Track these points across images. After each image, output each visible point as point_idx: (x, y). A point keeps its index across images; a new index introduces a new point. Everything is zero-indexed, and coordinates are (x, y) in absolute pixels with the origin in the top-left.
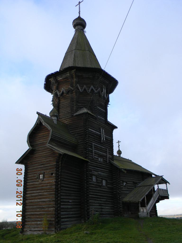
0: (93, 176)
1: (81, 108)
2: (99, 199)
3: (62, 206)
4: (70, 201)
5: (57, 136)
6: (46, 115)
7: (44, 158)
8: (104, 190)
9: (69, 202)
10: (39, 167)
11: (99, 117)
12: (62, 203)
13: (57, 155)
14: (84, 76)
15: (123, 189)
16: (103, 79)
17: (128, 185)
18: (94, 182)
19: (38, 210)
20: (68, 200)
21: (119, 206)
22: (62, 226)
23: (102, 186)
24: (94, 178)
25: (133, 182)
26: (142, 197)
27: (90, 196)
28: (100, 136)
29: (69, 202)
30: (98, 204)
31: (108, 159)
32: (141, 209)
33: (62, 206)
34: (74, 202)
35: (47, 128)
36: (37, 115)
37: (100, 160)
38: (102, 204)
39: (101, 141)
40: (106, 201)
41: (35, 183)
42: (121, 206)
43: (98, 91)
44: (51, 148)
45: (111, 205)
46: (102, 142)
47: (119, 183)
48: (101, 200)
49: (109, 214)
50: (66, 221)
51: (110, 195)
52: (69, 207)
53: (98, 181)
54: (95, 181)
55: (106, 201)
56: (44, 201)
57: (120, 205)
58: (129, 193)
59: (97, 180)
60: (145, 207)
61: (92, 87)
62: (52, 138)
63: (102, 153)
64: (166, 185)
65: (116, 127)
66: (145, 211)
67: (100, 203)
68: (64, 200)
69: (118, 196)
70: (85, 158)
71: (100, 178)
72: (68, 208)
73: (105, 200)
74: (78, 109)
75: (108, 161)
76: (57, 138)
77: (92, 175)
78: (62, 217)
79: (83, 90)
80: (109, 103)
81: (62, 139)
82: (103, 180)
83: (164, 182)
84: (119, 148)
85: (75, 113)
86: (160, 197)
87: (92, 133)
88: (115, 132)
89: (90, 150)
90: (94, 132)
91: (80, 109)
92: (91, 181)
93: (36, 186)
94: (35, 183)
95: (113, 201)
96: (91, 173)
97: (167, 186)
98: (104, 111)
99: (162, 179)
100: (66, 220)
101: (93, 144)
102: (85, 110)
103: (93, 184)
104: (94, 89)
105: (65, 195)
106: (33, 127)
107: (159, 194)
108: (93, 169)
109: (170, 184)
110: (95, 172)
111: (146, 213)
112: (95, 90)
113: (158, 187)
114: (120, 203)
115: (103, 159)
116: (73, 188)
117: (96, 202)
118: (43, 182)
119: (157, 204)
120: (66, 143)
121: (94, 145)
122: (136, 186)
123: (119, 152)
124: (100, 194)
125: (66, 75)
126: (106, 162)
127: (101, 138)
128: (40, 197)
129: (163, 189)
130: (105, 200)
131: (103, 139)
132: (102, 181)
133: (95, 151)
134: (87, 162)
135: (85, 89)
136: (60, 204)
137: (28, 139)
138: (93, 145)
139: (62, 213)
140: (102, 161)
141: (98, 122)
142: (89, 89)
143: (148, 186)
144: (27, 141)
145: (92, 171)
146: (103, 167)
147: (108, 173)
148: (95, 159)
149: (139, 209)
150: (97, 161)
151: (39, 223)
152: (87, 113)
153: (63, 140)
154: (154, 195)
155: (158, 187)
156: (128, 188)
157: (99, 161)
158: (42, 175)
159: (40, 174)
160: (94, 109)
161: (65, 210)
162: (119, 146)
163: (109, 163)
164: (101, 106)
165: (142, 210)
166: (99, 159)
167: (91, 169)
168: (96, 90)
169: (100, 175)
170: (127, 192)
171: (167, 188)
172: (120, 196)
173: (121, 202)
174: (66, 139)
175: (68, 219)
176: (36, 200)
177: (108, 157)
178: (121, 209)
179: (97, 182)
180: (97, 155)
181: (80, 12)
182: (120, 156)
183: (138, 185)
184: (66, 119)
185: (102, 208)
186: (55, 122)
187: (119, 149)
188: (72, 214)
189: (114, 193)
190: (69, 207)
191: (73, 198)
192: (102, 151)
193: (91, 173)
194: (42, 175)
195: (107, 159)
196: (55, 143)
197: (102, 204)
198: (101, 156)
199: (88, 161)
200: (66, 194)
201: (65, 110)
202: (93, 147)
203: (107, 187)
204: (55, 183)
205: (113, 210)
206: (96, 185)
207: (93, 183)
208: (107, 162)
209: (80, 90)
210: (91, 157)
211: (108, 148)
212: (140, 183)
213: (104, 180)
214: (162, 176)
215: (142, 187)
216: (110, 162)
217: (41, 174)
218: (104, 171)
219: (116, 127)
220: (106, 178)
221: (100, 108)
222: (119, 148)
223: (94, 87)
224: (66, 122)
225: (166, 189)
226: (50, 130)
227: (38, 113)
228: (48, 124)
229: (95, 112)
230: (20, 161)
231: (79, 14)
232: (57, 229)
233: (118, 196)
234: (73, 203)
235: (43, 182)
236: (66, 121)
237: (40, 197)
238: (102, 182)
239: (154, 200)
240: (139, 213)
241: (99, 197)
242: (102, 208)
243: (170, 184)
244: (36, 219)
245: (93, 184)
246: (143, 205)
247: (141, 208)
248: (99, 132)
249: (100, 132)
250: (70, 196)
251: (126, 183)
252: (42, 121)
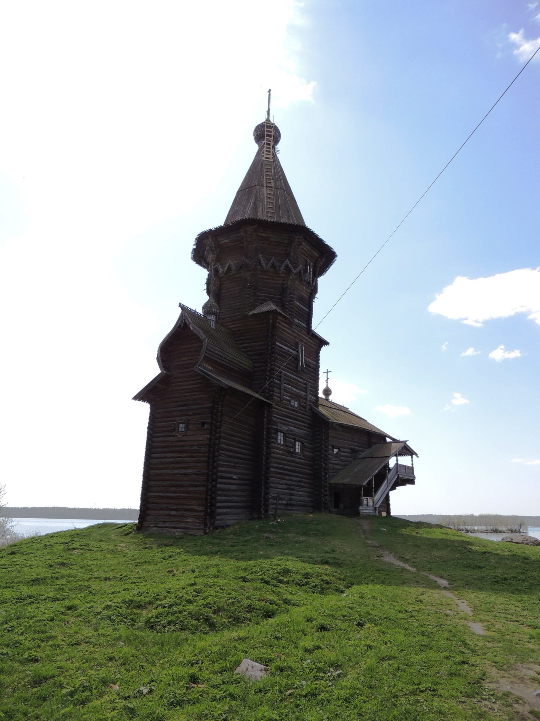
0: (279, 433)
1: (263, 301)
2: (287, 477)
3: (219, 486)
4: (234, 477)
5: (216, 352)
6: (197, 311)
7: (189, 394)
8: (297, 460)
9: (231, 478)
10: (179, 409)
11: (296, 321)
12: (219, 480)
13: (215, 388)
14: (272, 240)
15: (333, 461)
16: (308, 247)
17: (342, 454)
18: (280, 444)
19: (174, 489)
20: (230, 475)
21: (323, 491)
22: (217, 522)
23: (294, 452)
24: (280, 438)
25: (352, 449)
26: (367, 478)
27: (272, 469)
28: (296, 358)
29: (231, 478)
30: (285, 487)
31: (308, 403)
32: (364, 500)
33: (219, 486)
34: (240, 479)
35: (199, 335)
36: (179, 311)
37: (292, 404)
38: (292, 487)
39: (297, 367)
40: (299, 481)
41: (170, 439)
42: (327, 493)
43: (297, 270)
44: (203, 374)
45: (309, 490)
46: (299, 369)
47: (326, 449)
48: (292, 478)
49: (302, 506)
50: (224, 514)
51: (308, 471)
52: (232, 487)
53: (287, 444)
54: (282, 442)
55: (299, 481)
56: (185, 474)
57: (326, 491)
58: (342, 470)
59: (285, 440)
60: (371, 496)
61: (287, 261)
62: (207, 355)
63: (298, 391)
64: (412, 457)
65: (326, 343)
66: (371, 503)
67: (290, 485)
68: (224, 474)
69: (323, 474)
70: (267, 399)
71: (291, 438)
72: (229, 490)
73: (298, 479)
74: (256, 302)
75: (308, 407)
76: (215, 355)
77: (277, 431)
78: (218, 504)
79: (268, 267)
80: (317, 296)
81: (225, 360)
82: (297, 443)
83: (408, 452)
84: (327, 383)
85: (251, 310)
86: (399, 481)
87: (281, 351)
88: (324, 351)
89: (277, 384)
90: (285, 349)
91: (262, 303)
92: (274, 443)
93: (170, 444)
94: (170, 439)
95: (312, 482)
96: (275, 427)
97: (412, 461)
98: (306, 311)
99: (405, 446)
100: (225, 510)
101: (283, 372)
102: (272, 307)
103: (278, 449)
104: (290, 265)
105: (225, 465)
106: (171, 332)
107: (398, 475)
108: (279, 421)
109: (418, 457)
110: (282, 425)
111: (373, 508)
112: (293, 269)
113: (397, 460)
114: (325, 486)
115: (299, 403)
116: (240, 453)
117: (282, 482)
118: (185, 438)
119: (390, 492)
120: (232, 367)
121: (285, 375)
122: (356, 456)
123: (327, 392)
124: (289, 468)
125: (238, 235)
126: (304, 409)
127: (297, 364)
128: (179, 465)
129: (405, 466)
130: (298, 479)
131: (302, 364)
132: (294, 444)
133: (285, 387)
134: (270, 406)
135: (273, 266)
136: (216, 481)
137: (159, 354)
138: (282, 375)
139: (218, 498)
140: (296, 406)
141: (293, 331)
142: (280, 267)
143: (379, 457)
144: (158, 359)
145: (278, 424)
147: (306, 429)
148: (284, 401)
149: (360, 499)
151: (173, 513)
152: (275, 312)
153: (227, 361)
154: (389, 476)
155: (397, 460)
156: (341, 460)
157: (292, 406)
158: (184, 425)
159: (180, 423)
160: (287, 305)
161: (225, 493)
162: (328, 379)
163: (309, 411)
164: (301, 299)
165: (365, 502)
166: (293, 401)
167: (276, 419)
168: (295, 268)
169: (291, 432)
170: (340, 467)
171: (412, 464)
172: (326, 474)
173: (327, 485)
174: (232, 360)
175: (229, 510)
176: (169, 471)
177: (309, 399)
178: (326, 498)
179: (285, 445)
181: (269, 109)
182: (327, 399)
183: (360, 455)
184: (234, 321)
185: (291, 494)
186: (211, 325)
187: (327, 385)
188: (236, 502)
189: (316, 467)
190: (232, 487)
191: (239, 471)
192: (299, 387)
193: (275, 427)
194: (184, 425)
195: (306, 403)
196: (211, 366)
197: (292, 487)
198: (295, 396)
199: (272, 405)
200: (227, 464)
201: (231, 302)
202: (282, 379)
203: (303, 456)
204: (207, 442)
205: (310, 499)
206: (283, 450)
207: (279, 446)
208: (305, 408)
209: (264, 265)
210: (278, 397)
211: (310, 382)
212: (363, 452)
213: (298, 441)
214: (405, 442)
215: (366, 460)
216: (311, 409)
217: (182, 423)
218: (300, 425)
219: (326, 343)
220: (302, 438)
221: (299, 304)
222: (327, 383)
223: (290, 263)
224: (233, 326)
225: (411, 466)
226: (205, 339)
227: (180, 306)
228: (199, 327)
229: (289, 311)
230: (141, 396)
231: (268, 114)
232: (208, 526)
233: (323, 474)
234: (238, 482)
235: (185, 438)
236: (234, 324)
237: (179, 465)
238: (294, 446)
239: (388, 484)
240: (361, 508)
241: (286, 472)
242: (291, 494)
243: (418, 457)
244: (169, 506)
245: (278, 449)
246: (370, 491)
247: (363, 497)
248: (294, 350)
249: (298, 352)
250: (234, 467)
251: (339, 450)
252: (189, 321)
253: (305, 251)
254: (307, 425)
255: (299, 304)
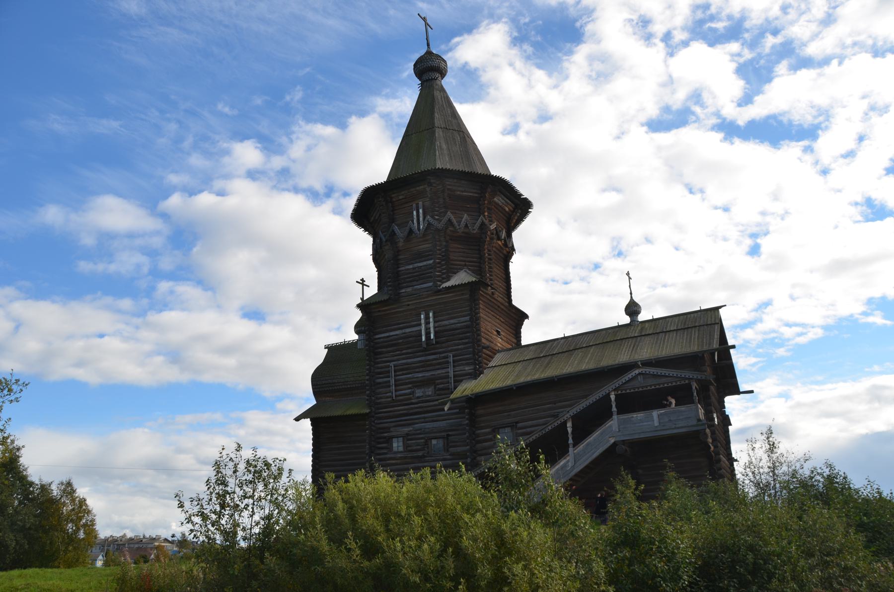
16: (403, 193)
77: (389, 440)
96: (386, 435)
120: (349, 386)
141: (408, 305)
146: (432, 408)
150: (411, 399)
157: (418, 397)
180: (410, 386)
187: (631, 297)
203: (450, 455)
206: (405, 458)
231: (428, 45)
251: (513, 426)
253: (403, 199)
254: (458, 410)
255: (411, 267)
